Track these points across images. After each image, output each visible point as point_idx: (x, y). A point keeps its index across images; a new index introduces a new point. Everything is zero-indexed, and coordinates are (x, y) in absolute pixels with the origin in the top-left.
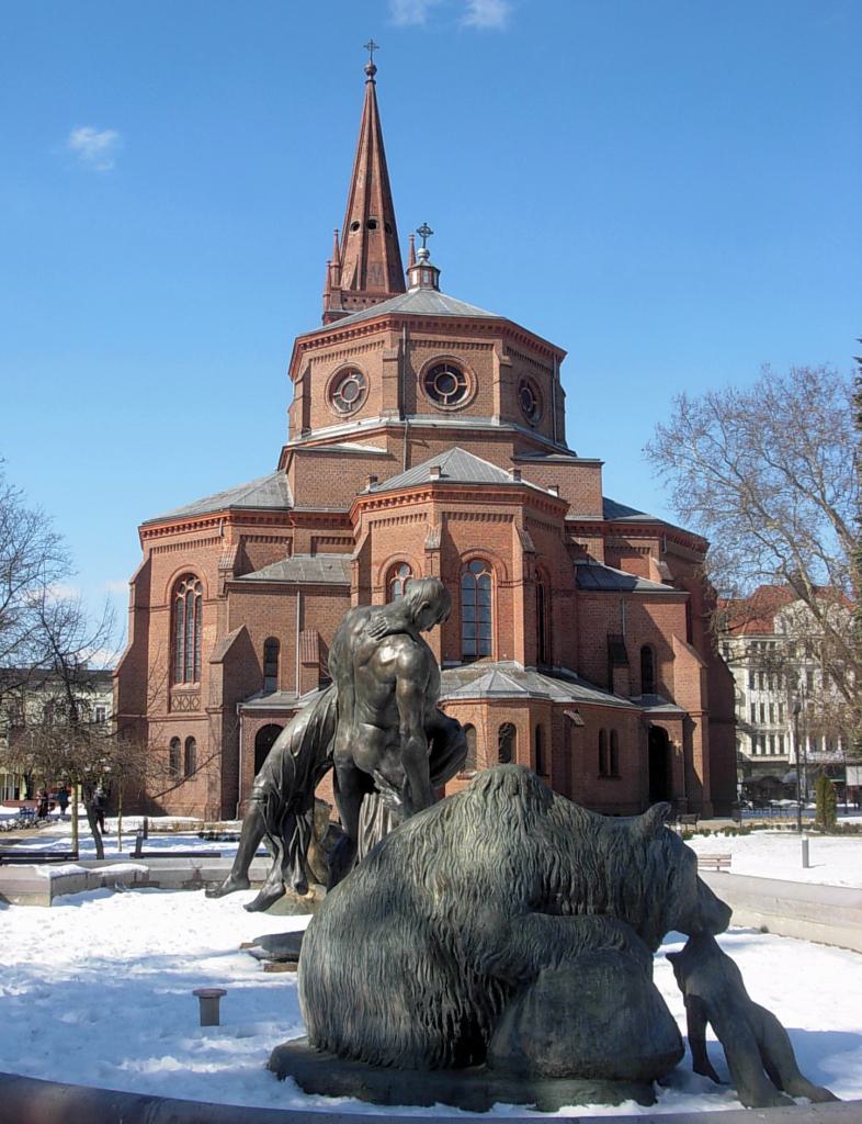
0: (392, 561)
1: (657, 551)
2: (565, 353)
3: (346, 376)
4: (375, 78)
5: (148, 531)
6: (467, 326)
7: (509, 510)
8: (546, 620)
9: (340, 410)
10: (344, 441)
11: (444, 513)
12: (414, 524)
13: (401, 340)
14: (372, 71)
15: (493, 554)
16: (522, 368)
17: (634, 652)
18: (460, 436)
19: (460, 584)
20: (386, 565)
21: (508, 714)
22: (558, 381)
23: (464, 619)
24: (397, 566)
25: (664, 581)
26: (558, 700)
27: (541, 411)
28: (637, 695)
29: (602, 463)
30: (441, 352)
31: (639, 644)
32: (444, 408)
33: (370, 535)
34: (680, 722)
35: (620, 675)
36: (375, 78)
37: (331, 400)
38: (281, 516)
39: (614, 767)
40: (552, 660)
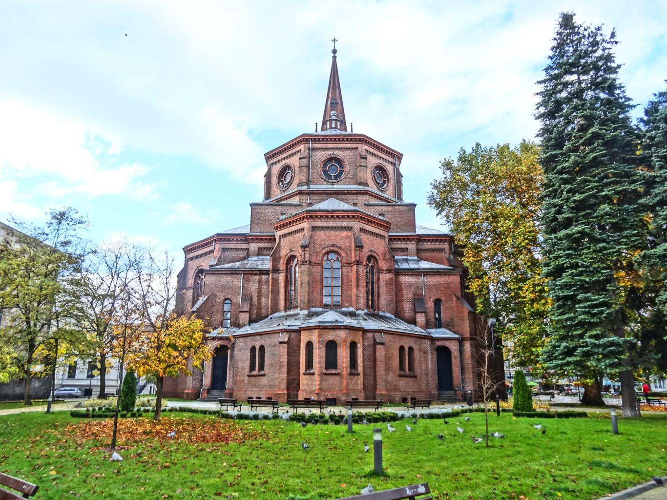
0: (288, 255)
1: (447, 250)
2: (402, 155)
3: (286, 170)
4: (336, 55)
5: (188, 250)
6: (343, 139)
7: (350, 224)
10: (281, 200)
11: (313, 227)
13: (309, 148)
14: (335, 52)
15: (340, 248)
16: (373, 161)
17: (430, 304)
18: (337, 194)
19: (322, 267)
20: (287, 258)
21: (330, 336)
22: (398, 170)
23: (325, 285)
24: (292, 258)
25: (450, 266)
26: (366, 328)
27: (388, 183)
28: (433, 328)
29: (416, 205)
30: (331, 152)
31: (433, 299)
32: (331, 181)
33: (279, 243)
34: (456, 343)
35: (421, 318)
36: (336, 55)
37: (279, 183)
38: (245, 238)
39: (411, 368)
40: (379, 308)
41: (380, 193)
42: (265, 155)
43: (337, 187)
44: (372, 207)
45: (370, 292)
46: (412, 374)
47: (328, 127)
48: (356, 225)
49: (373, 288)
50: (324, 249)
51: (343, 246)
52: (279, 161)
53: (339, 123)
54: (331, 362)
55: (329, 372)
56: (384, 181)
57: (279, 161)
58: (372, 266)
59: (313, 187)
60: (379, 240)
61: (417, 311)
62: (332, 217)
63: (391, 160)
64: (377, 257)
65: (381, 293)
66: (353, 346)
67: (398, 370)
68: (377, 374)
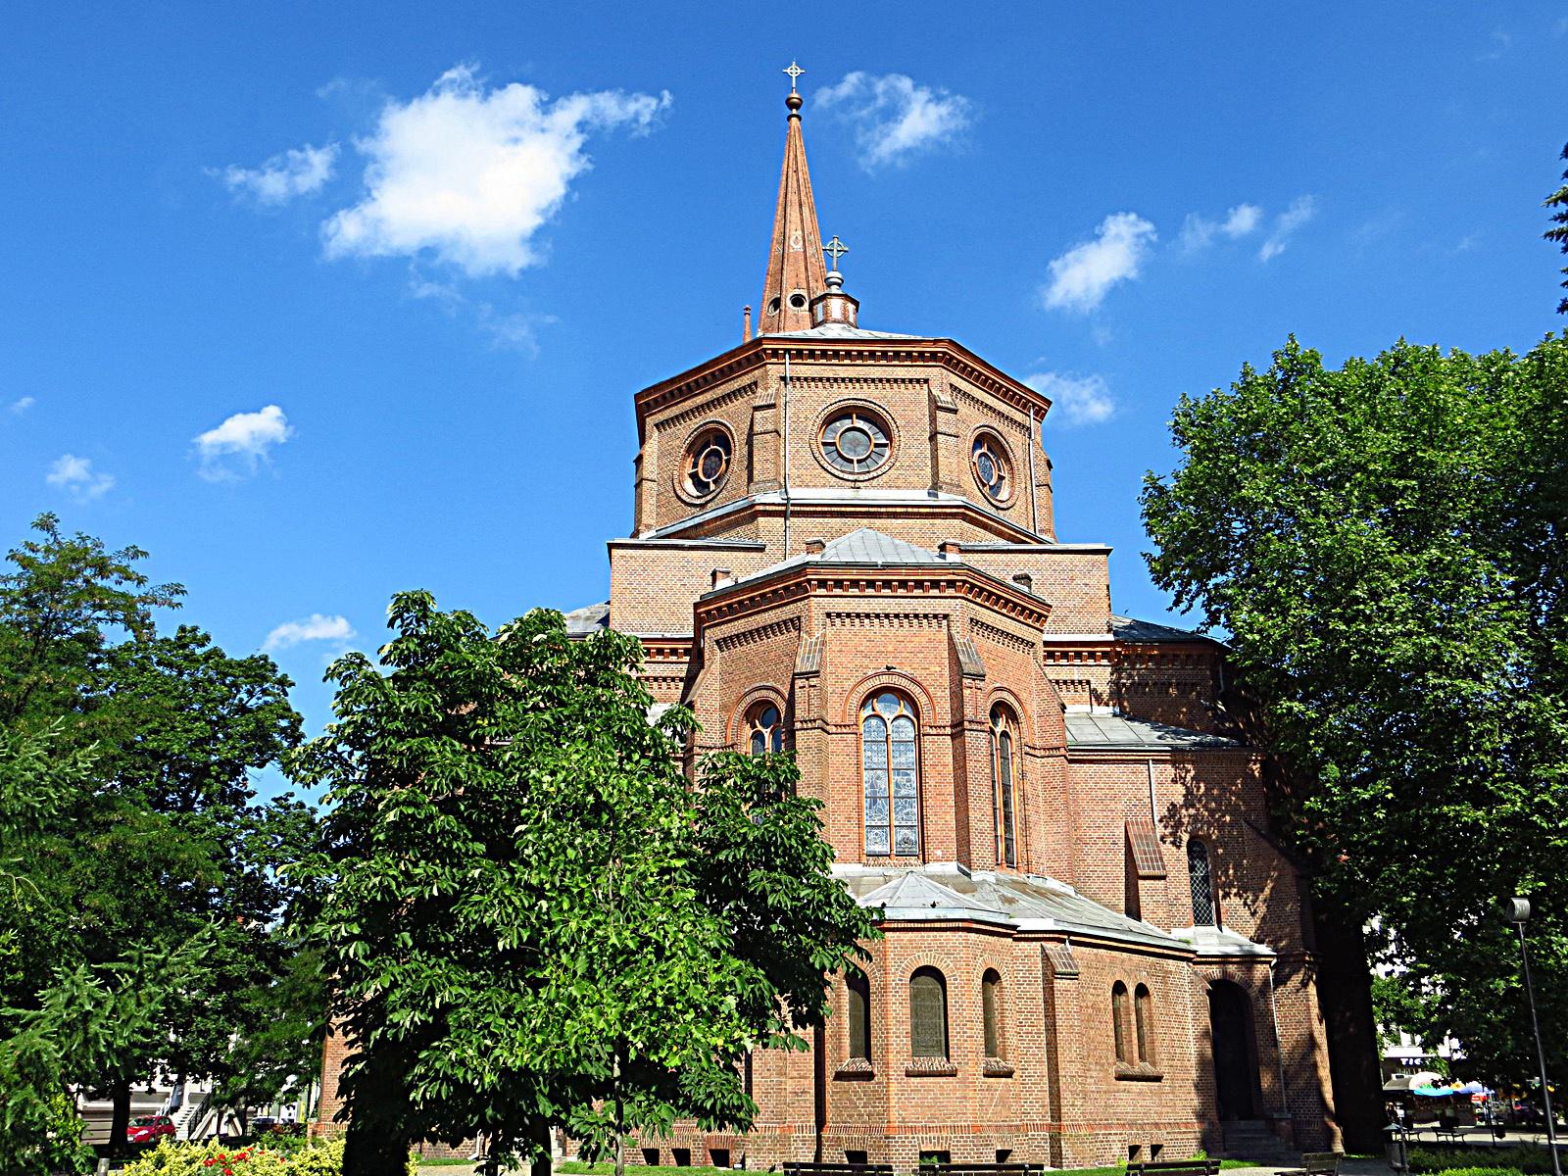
8: (1015, 797)
9: (695, 493)
11: (829, 615)
12: (779, 639)
15: (913, 681)
28: (1187, 926)
41: (992, 511)
42: (637, 397)
43: (870, 494)
44: (977, 556)
45: (1000, 814)
46: (1148, 1068)
47: (820, 318)
48: (957, 607)
49: (1006, 804)
50: (862, 682)
51: (918, 674)
52: (683, 416)
53: (851, 307)
54: (932, 1032)
55: (924, 1064)
56: (1001, 478)
57: (683, 416)
58: (1004, 734)
59: (795, 493)
60: (1018, 654)
61: (1141, 872)
62: (887, 584)
63: (1018, 416)
64: (1016, 705)
65: (1033, 818)
66: (991, 977)
67: (1112, 1057)
68: (1062, 1073)
